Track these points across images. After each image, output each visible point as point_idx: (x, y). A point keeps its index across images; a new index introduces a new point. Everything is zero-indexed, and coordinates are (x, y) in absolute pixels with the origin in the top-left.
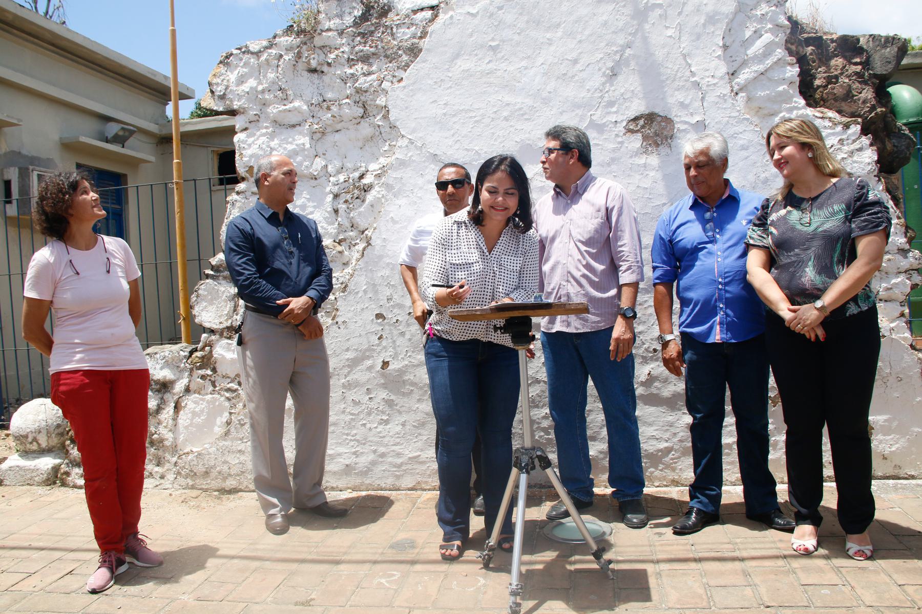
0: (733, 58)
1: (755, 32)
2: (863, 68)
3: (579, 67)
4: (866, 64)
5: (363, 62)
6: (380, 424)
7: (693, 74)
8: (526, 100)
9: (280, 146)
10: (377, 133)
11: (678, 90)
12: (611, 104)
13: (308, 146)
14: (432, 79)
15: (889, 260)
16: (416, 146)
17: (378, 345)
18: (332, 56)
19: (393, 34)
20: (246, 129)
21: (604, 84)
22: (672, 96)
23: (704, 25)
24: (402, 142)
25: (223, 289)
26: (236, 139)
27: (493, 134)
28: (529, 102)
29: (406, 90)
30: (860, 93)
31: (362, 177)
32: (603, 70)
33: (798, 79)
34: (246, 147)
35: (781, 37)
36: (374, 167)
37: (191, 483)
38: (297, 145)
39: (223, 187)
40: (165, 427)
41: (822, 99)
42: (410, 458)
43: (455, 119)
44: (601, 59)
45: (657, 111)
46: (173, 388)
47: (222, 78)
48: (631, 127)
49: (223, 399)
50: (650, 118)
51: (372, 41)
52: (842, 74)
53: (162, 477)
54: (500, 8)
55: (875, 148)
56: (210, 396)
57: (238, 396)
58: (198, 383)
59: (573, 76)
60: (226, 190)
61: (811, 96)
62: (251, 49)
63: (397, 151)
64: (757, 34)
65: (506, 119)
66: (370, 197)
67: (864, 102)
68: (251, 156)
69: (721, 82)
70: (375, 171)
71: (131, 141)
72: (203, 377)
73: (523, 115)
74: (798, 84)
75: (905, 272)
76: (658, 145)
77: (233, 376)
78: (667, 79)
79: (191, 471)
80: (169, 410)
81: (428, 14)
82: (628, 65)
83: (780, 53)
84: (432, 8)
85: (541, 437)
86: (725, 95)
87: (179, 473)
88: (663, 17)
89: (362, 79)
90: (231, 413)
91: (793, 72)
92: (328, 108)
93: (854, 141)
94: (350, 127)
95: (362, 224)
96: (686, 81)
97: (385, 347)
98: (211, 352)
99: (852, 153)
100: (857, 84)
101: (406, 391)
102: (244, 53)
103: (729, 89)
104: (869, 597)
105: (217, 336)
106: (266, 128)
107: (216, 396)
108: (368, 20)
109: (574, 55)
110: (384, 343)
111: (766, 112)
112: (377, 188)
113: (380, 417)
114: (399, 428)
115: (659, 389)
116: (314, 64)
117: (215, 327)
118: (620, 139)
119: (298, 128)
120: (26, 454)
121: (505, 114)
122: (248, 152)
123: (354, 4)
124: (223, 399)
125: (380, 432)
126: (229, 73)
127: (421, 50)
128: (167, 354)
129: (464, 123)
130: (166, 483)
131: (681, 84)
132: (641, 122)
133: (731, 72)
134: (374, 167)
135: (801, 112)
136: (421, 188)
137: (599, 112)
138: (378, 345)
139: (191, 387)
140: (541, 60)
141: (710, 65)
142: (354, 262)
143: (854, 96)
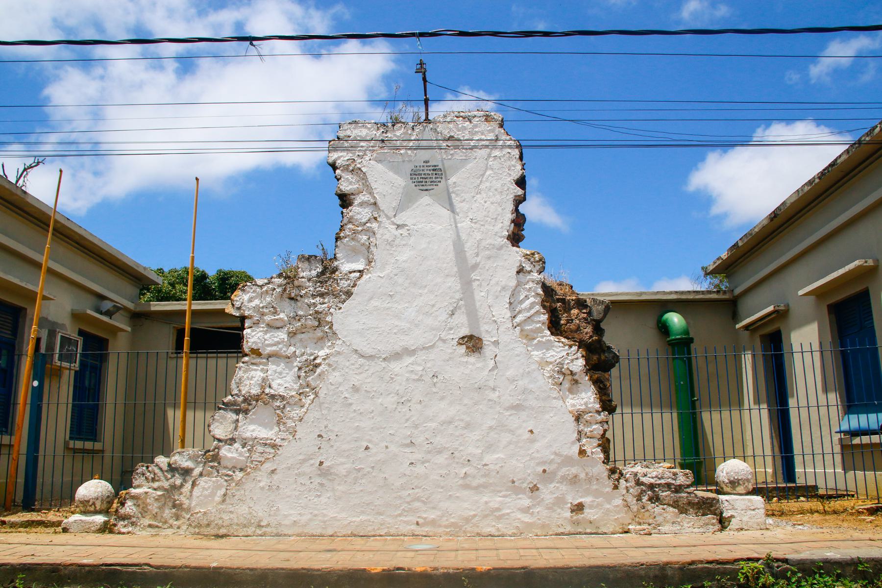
3: (435, 309)
4: (589, 313)
12: (451, 329)
18: (304, 292)
24: (339, 342)
26: (245, 332)
28: (408, 325)
31: (314, 359)
35: (538, 300)
36: (322, 353)
37: (197, 530)
50: (471, 337)
53: (179, 528)
54: (396, 275)
57: (232, 479)
63: (336, 346)
64: (527, 297)
66: (318, 370)
71: (117, 316)
72: (212, 467)
80: (188, 485)
81: (358, 274)
83: (538, 307)
84: (360, 271)
87: (190, 525)
88: (480, 285)
89: (319, 306)
91: (544, 317)
92: (299, 320)
95: (313, 384)
99: (572, 361)
109: (433, 302)
110: (321, 451)
114: (326, 500)
116: (293, 295)
117: (222, 437)
120: (84, 513)
134: (322, 353)
140: (415, 304)
141: (502, 312)
142: (307, 405)
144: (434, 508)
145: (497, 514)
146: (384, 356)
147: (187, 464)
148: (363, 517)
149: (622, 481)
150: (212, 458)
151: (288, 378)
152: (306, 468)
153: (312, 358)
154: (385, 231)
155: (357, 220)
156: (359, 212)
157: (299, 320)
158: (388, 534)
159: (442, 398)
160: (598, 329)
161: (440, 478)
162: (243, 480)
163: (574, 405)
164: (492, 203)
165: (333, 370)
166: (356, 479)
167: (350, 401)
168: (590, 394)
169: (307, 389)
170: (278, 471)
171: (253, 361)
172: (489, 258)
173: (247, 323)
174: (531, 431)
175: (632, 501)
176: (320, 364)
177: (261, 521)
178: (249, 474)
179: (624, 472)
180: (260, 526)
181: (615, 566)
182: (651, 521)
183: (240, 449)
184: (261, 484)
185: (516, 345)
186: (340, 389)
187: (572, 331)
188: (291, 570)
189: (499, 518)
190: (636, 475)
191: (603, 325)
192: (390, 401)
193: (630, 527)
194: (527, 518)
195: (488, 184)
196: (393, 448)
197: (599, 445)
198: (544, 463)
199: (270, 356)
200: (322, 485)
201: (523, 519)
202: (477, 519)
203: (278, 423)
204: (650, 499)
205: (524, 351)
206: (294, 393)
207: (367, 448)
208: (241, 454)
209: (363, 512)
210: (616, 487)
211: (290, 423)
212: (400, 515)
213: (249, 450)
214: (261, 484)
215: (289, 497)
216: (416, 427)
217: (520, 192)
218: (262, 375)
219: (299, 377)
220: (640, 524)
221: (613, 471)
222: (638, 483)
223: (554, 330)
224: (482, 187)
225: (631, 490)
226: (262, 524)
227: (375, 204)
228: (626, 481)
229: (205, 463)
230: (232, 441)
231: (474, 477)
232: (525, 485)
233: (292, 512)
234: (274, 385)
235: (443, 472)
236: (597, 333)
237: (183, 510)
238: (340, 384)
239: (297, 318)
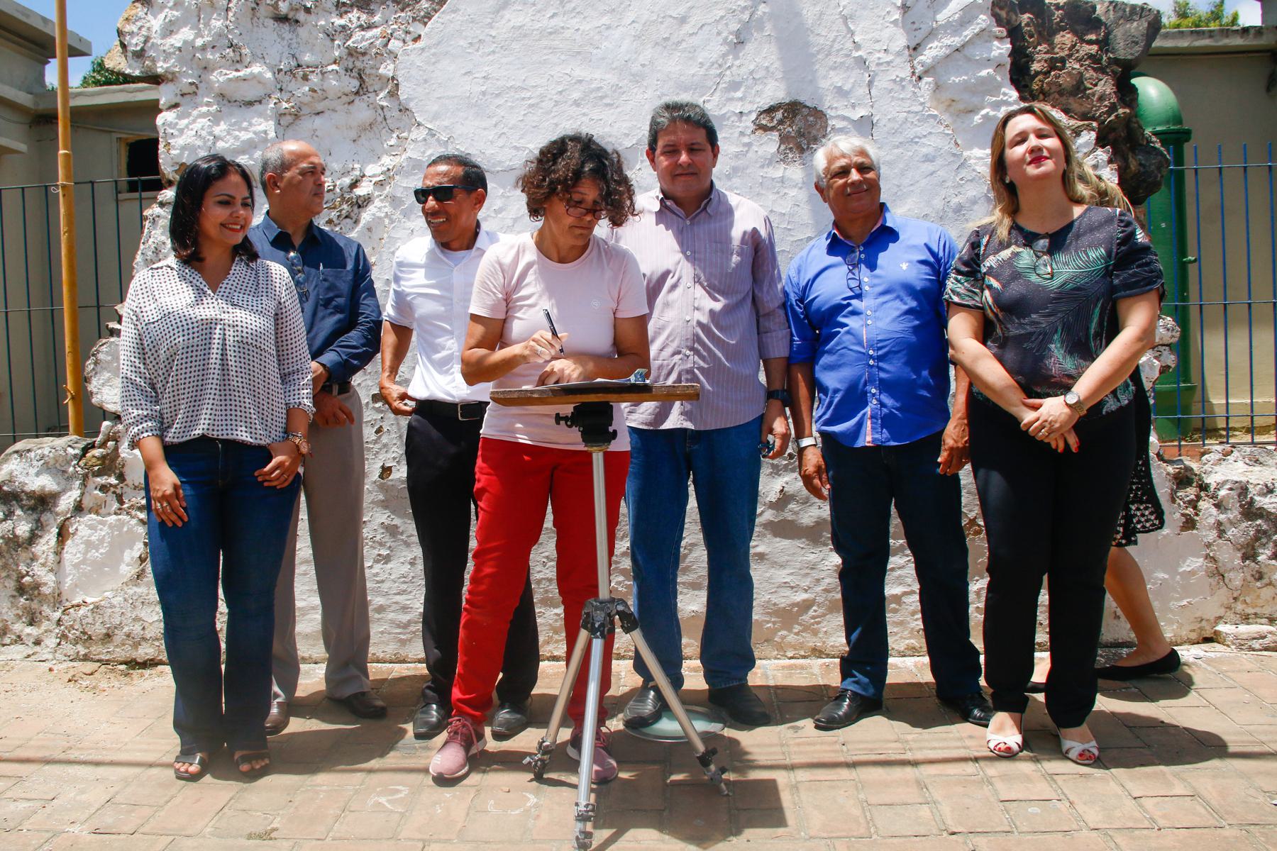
3: (687, 28)
6: (377, 561)
7: (857, 46)
8: (608, 76)
9: (229, 133)
10: (380, 119)
11: (835, 68)
12: (735, 86)
13: (272, 134)
14: (465, 38)
16: (438, 140)
17: (375, 442)
20: (176, 106)
21: (724, 56)
22: (825, 77)
26: (160, 120)
27: (556, 125)
28: (612, 78)
29: (425, 54)
31: (354, 185)
32: (724, 34)
33: (1008, 61)
34: (176, 133)
36: (372, 169)
37: (83, 651)
38: (255, 133)
39: (136, 195)
40: (43, 565)
41: (1042, 91)
43: (500, 101)
44: (722, 17)
45: (802, 99)
46: (55, 505)
47: (139, 24)
48: (764, 122)
49: (134, 521)
50: (793, 109)
53: (37, 643)
55: (1115, 166)
56: (114, 517)
58: (96, 497)
59: (679, 43)
60: (141, 199)
65: (577, 103)
66: (366, 216)
68: (184, 148)
69: (898, 60)
70: (374, 176)
72: (104, 488)
73: (602, 98)
74: (1008, 67)
78: (818, 52)
79: (84, 633)
82: (761, 28)
83: (984, 20)
85: (619, 583)
86: (902, 80)
89: (358, 35)
91: (1002, 49)
92: (305, 78)
97: (385, 445)
98: (116, 449)
103: (908, 71)
104: (1093, 816)
106: (207, 105)
107: (124, 517)
109: (681, 10)
110: (385, 439)
111: (961, 107)
112: (377, 203)
113: (376, 552)
115: (796, 513)
118: (746, 140)
119: (257, 106)
121: (576, 95)
122: (178, 142)
124: (134, 521)
125: (377, 575)
126: (150, 17)
128: (46, 453)
129: (512, 108)
130: (44, 652)
131: (839, 60)
132: (779, 115)
134: (372, 169)
137: (716, 98)
138: (375, 442)
139: (87, 503)
140: (630, 16)
147: (45, 483)
153: (347, 181)
175: (1229, 557)
176: (367, 200)
179: (1211, 480)
185: (923, 129)
193: (1221, 628)
205: (947, 146)
220: (1246, 619)
222: (1250, 512)
225: (1231, 532)
228: (1218, 506)
229: (85, 477)
237: (43, 599)
239: (300, 72)
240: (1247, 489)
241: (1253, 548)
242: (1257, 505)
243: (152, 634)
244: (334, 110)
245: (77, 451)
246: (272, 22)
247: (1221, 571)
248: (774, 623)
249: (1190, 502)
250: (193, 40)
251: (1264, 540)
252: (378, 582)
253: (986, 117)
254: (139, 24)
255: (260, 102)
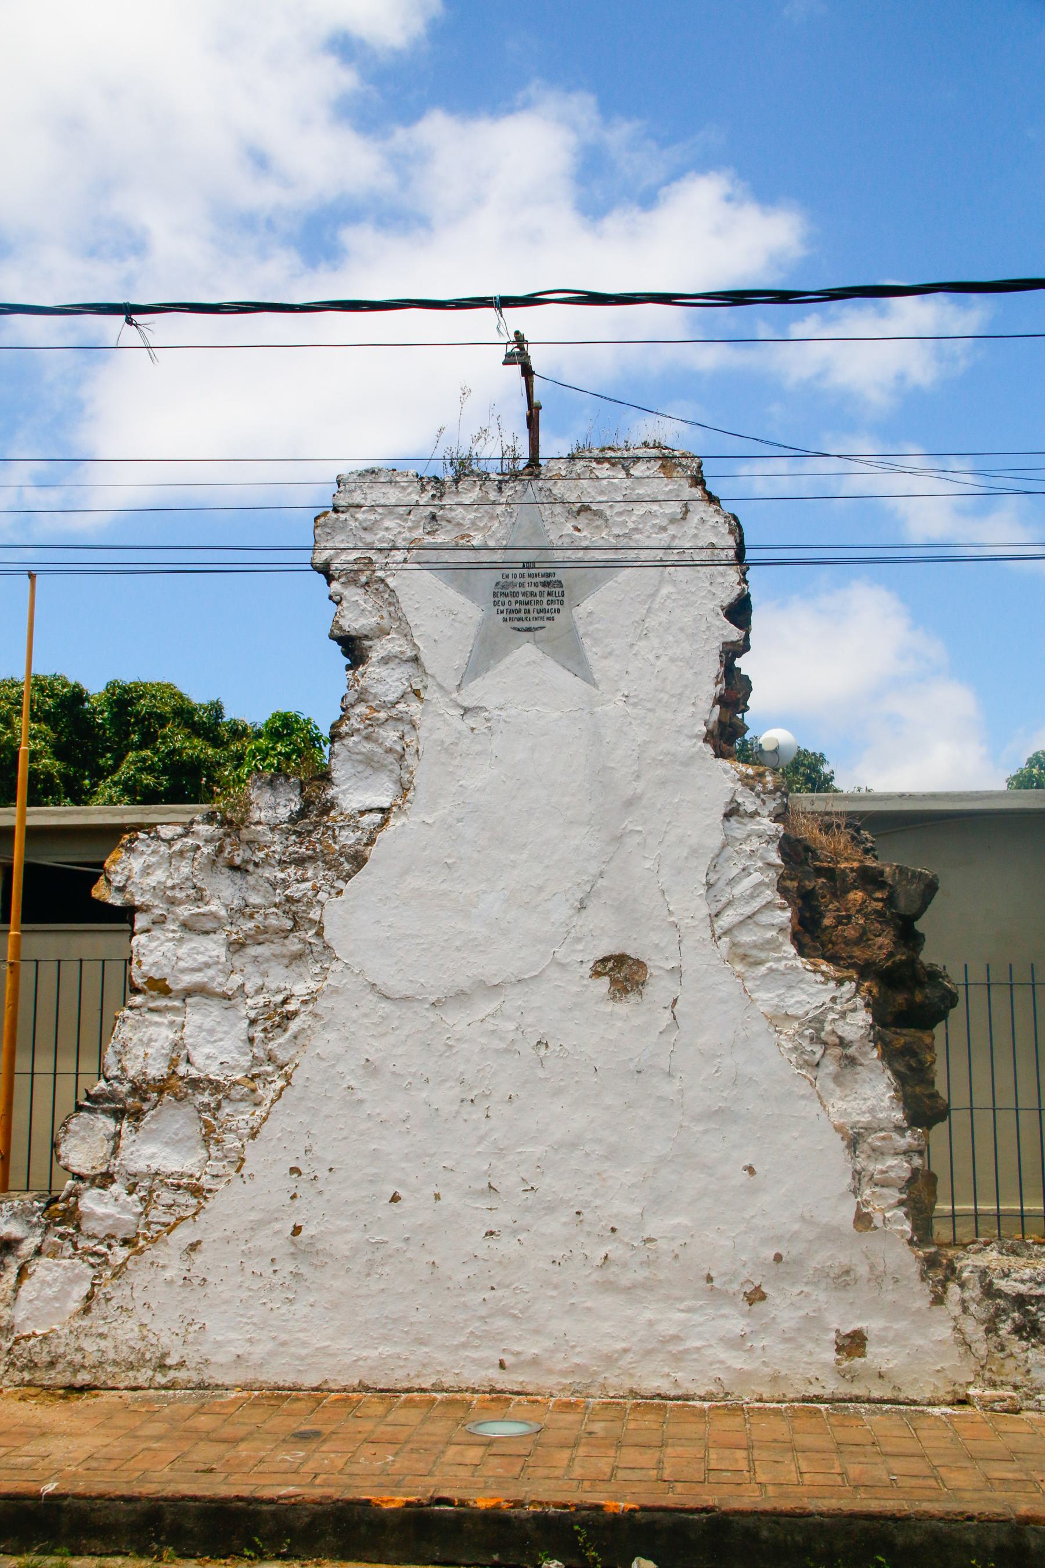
0: (718, 898)
1: (744, 870)
2: (885, 906)
5: (297, 865)
6: (284, 1303)
11: (653, 930)
12: (578, 940)
13: (223, 959)
15: (883, 1138)
16: (352, 972)
17: (289, 1205)
18: (261, 855)
19: (334, 837)
20: (148, 931)
21: (571, 917)
23: (686, 858)
24: (335, 966)
25: (101, 1125)
27: (442, 965)
30: (879, 936)
31: (285, 1002)
36: (300, 989)
37: (27, 1376)
42: (317, 1349)
45: (628, 952)
46: (17, 1249)
47: (123, 865)
50: (620, 960)
51: (310, 841)
52: (858, 912)
54: (460, 820)
56: (68, 1261)
57: (106, 1262)
58: (54, 1244)
61: (818, 937)
62: (162, 835)
63: (330, 975)
65: (458, 949)
66: (294, 1026)
67: (880, 948)
72: (62, 1236)
74: (790, 930)
75: (905, 1153)
76: (628, 992)
77: (102, 1236)
79: (31, 1361)
81: (377, 817)
83: (770, 894)
84: (382, 810)
85: (475, 1328)
87: (13, 1364)
88: (643, 845)
89: (295, 887)
90: (93, 1285)
91: (784, 916)
92: (251, 916)
93: (849, 1000)
94: (276, 941)
95: (282, 1056)
96: (663, 920)
97: (298, 1208)
98: (76, 1203)
99: (843, 1015)
100: (876, 925)
101: (319, 1263)
102: (153, 838)
103: (710, 933)
105: (88, 1184)
107: (76, 1261)
108: (305, 817)
110: (297, 1202)
112: (302, 1017)
116: (238, 861)
117: (84, 1171)
118: (585, 982)
119: (212, 935)
121: (458, 943)
123: (293, 797)
124: (86, 1265)
125: (283, 1315)
127: (365, 860)
131: (657, 923)
132: (610, 965)
133: (713, 913)
135: (790, 963)
136: (355, 1022)
138: (289, 1205)
141: (691, 905)
143: (868, 940)
144: (536, 1332)
145: (674, 1348)
146: (433, 998)
148: (386, 1350)
149: (953, 1288)
150: (61, 1214)
151: (227, 1043)
152: (264, 1240)
153: (280, 998)
154: (437, 722)
155: (375, 696)
156: (384, 679)
157: (251, 916)
158: (438, 1388)
159: (558, 1092)
160: (908, 935)
161: (552, 1266)
162: (129, 1265)
163: (844, 1113)
164: (672, 660)
165: (324, 1027)
166: (371, 1264)
167: (360, 1095)
168: (882, 1087)
169: (267, 1072)
170: (204, 1246)
171: (152, 1005)
172: (663, 783)
173: (141, 921)
174: (750, 1170)
175: (974, 1331)
177: (165, 1355)
178: (140, 1252)
179: (958, 1265)
180: (162, 1367)
181: (907, 1518)
182: (1018, 1379)
183: (124, 1196)
184: (168, 1274)
186: (340, 1068)
187: (847, 942)
188: (212, 1500)
189: (678, 1358)
190: (984, 1273)
191: (919, 926)
192: (445, 1096)
193: (972, 1391)
194: (738, 1361)
195: (663, 617)
196: (449, 1198)
197: (901, 1203)
198: (779, 1239)
199: (188, 993)
200: (296, 1275)
201: (729, 1363)
202: (629, 1358)
203: (206, 1140)
204: (1018, 1330)
206: (239, 1076)
207: (395, 1198)
208: (124, 1208)
209: (385, 1339)
210: (938, 1300)
211: (231, 1141)
212: (464, 1346)
213: (142, 1199)
214: (168, 1274)
215: (226, 1302)
216: (501, 1152)
217: (734, 634)
218: (171, 1036)
219: (251, 1040)
220: (993, 1385)
221: (931, 1262)
222: (990, 1292)
223: (807, 939)
224: (651, 622)
225: (973, 1307)
226: (169, 1361)
227: (416, 659)
228: (962, 1285)
229: (47, 1226)
230: (106, 1179)
231: (625, 1265)
232: (735, 1287)
233: (232, 1335)
234: (197, 1058)
235: (558, 1253)
236: (906, 945)
238: (338, 1058)
240: (986, 1273)
241: (995, 1324)
242: (995, 1287)
243: (91, 1363)
244: (272, 942)
245: (42, 1205)
246: (227, 870)
247: (968, 1340)
248: (598, 1366)
249: (939, 1281)
250: (165, 882)
251: (1004, 1318)
252: (284, 1321)
253: (771, 970)
254: (123, 865)
255: (215, 932)
